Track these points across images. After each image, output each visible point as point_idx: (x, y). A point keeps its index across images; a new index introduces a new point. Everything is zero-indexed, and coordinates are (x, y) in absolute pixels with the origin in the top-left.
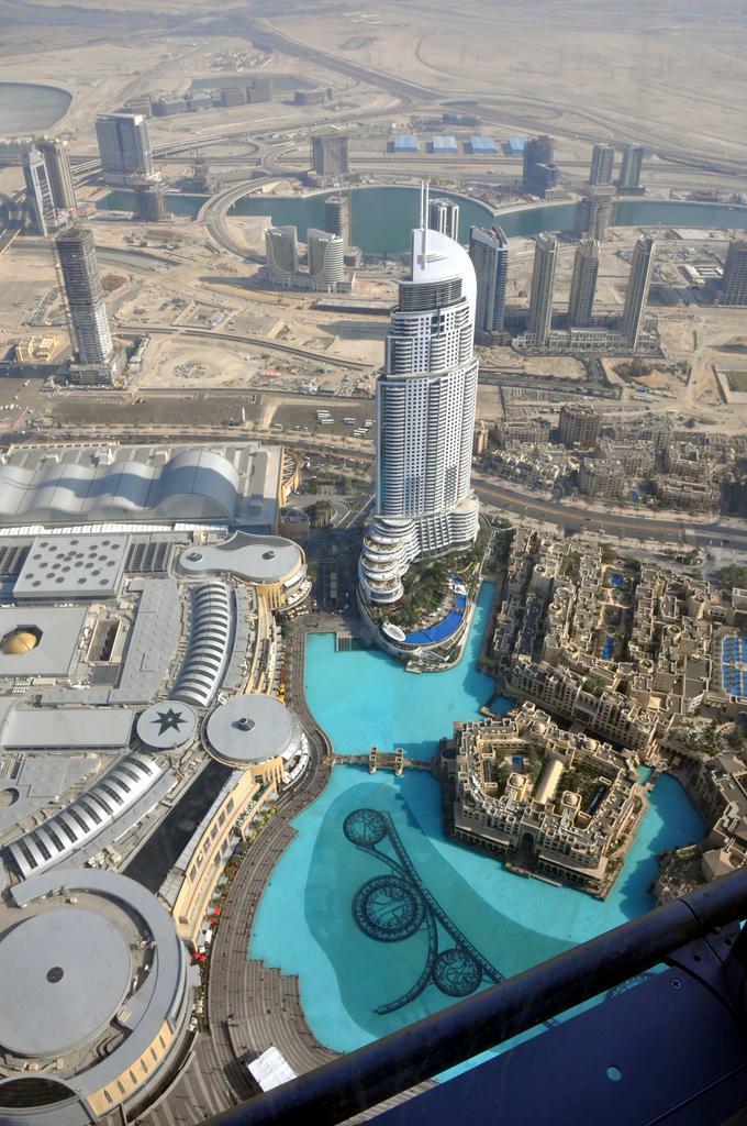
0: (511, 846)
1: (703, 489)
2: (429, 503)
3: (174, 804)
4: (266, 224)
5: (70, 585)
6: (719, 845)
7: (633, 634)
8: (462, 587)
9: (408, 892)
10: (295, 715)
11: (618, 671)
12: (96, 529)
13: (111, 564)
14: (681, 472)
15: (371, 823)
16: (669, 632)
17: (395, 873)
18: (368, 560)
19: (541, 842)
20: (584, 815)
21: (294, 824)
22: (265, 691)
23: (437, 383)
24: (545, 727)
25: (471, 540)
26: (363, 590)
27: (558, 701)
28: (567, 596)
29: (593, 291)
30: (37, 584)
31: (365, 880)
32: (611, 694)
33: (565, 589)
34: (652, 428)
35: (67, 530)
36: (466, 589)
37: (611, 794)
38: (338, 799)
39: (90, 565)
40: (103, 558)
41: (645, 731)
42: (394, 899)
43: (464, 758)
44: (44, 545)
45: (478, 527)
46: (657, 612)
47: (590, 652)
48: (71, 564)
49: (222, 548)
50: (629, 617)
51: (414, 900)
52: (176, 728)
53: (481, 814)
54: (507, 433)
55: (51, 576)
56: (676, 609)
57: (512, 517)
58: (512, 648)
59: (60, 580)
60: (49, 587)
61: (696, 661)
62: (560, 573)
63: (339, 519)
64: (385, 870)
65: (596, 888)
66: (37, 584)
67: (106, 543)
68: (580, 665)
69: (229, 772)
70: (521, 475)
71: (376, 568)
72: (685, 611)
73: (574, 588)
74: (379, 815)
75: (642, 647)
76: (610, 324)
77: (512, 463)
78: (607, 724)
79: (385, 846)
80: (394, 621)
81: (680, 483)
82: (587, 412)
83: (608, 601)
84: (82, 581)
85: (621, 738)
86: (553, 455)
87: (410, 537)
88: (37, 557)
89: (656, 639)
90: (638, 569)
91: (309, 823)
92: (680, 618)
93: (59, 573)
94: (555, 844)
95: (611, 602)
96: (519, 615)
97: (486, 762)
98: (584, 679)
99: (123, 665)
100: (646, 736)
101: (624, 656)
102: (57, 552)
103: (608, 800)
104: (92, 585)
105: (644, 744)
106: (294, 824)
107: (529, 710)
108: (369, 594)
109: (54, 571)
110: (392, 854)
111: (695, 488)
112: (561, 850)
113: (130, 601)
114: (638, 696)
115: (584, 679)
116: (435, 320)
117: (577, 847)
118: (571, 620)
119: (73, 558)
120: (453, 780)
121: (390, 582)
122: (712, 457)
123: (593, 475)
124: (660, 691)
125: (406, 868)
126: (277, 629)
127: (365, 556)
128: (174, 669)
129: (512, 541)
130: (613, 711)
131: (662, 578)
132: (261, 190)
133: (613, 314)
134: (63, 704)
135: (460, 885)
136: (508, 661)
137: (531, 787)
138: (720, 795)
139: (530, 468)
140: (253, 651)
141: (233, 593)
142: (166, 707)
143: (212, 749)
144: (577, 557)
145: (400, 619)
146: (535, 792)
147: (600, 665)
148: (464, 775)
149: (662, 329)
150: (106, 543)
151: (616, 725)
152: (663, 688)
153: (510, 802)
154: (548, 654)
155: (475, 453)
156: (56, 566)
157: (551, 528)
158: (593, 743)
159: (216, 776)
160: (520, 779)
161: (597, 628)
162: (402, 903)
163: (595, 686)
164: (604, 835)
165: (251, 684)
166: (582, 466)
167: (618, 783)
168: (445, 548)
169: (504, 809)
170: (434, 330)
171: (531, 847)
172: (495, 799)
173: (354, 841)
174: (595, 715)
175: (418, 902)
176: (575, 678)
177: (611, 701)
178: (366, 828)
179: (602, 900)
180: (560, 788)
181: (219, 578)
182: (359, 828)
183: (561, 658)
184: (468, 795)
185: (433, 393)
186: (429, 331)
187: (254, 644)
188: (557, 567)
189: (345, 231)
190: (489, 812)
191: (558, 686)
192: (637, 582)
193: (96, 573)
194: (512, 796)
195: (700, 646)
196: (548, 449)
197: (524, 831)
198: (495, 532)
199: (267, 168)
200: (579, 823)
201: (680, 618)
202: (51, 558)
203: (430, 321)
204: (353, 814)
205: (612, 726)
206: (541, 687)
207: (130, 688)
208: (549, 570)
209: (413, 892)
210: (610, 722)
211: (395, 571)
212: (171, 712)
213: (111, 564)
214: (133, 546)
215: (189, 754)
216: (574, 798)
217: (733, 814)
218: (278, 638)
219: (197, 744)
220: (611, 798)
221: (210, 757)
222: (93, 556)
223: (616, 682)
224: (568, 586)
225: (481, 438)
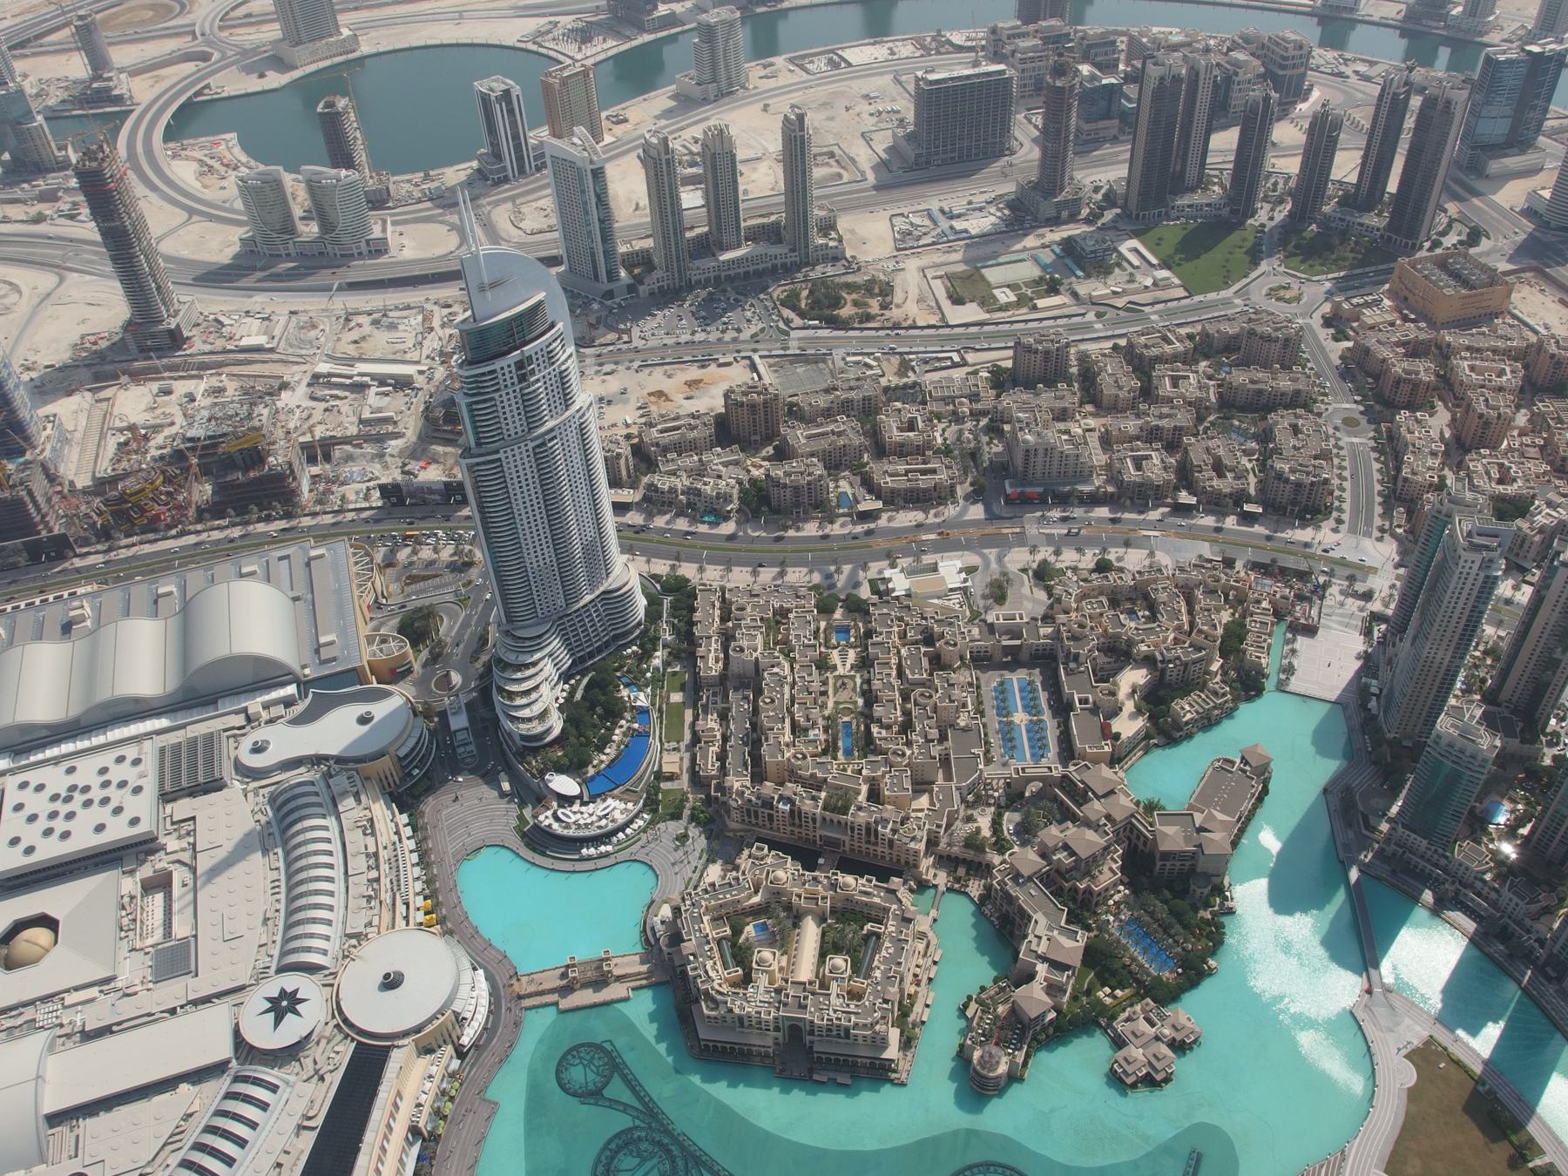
0: (777, 1044)
1: (934, 471)
2: (571, 596)
3: (319, 1122)
4: (229, 145)
5: (83, 839)
6: (1030, 977)
7: (876, 715)
8: (642, 696)
9: (659, 1143)
10: (453, 941)
11: (864, 772)
12: (97, 740)
13: (138, 790)
14: (902, 451)
15: (591, 1062)
16: (920, 700)
17: (637, 1122)
18: (511, 695)
19: (812, 1033)
20: (859, 983)
21: (491, 1094)
22: (406, 918)
23: (544, 444)
24: (786, 872)
25: (639, 624)
26: (509, 735)
27: (796, 830)
28: (781, 680)
29: (735, 182)
30: (30, 850)
31: (601, 1144)
32: (860, 809)
33: (776, 670)
34: (852, 394)
35: (50, 753)
36: (647, 697)
37: (887, 944)
38: (541, 1041)
39: (105, 801)
40: (123, 784)
41: (912, 845)
42: (644, 1160)
43: (688, 947)
44: (23, 785)
45: (645, 602)
46: (901, 674)
47: (825, 752)
48: (76, 805)
49: (296, 721)
50: (865, 687)
51: (668, 1151)
52: (297, 1013)
53: (729, 1016)
54: (657, 445)
55: (48, 832)
56: (925, 663)
57: (688, 570)
58: (723, 768)
59: (65, 835)
60: (51, 850)
61: (965, 730)
62: (766, 644)
63: (451, 628)
64: (623, 1121)
65: (895, 1071)
66: (30, 850)
67: (120, 760)
68: (813, 776)
69: (388, 1049)
70: (689, 505)
71: (519, 701)
72: (937, 662)
73: (787, 666)
74: (598, 1047)
75: (888, 727)
76: (770, 234)
77: (672, 490)
78: (864, 846)
79: (617, 1089)
80: (560, 770)
81: (901, 468)
82: (759, 394)
83: (835, 668)
84: (100, 828)
85: (885, 865)
86: (726, 464)
87: (556, 643)
88: (19, 807)
89: (907, 713)
90: (867, 613)
91: (510, 1089)
92: (931, 674)
93: (60, 825)
94: (829, 1030)
95: (841, 671)
96: (724, 717)
97: (719, 942)
98: (823, 794)
99: (195, 936)
100: (916, 852)
101: (868, 745)
102: (48, 793)
103: (884, 953)
104: (118, 831)
105: (916, 866)
106: (491, 1094)
107: (759, 854)
108: (517, 739)
109: (52, 824)
110: (627, 1097)
111: (924, 472)
112: (839, 1036)
113: (179, 838)
114: (898, 804)
115: (823, 794)
116: (520, 365)
117: (856, 1025)
118: (792, 714)
119: (76, 794)
120: (684, 973)
121: (543, 715)
122: (939, 417)
123: (785, 486)
124: (922, 785)
125: (650, 1111)
126: (404, 818)
127: (501, 690)
128: (270, 923)
129: (694, 610)
130: (868, 829)
131: (900, 619)
132: (207, 86)
133: (773, 218)
134: (119, 1024)
135: (723, 1111)
136: (721, 788)
137: (784, 964)
138: (1020, 907)
139: (698, 492)
140: (378, 868)
141: (329, 786)
142: (272, 988)
143: (351, 1026)
144: (783, 613)
145: (566, 761)
146: (792, 964)
147: (838, 769)
148: (695, 969)
149: (843, 224)
150: (120, 760)
151: (876, 844)
152: (927, 778)
153: (762, 989)
154: (771, 770)
155: (615, 483)
156: (53, 815)
157: (740, 577)
158: (850, 879)
159: (368, 1063)
160: (766, 954)
161: (826, 713)
162: (655, 1161)
163: (840, 803)
164: (886, 1001)
165: (387, 916)
166: (767, 476)
167: (892, 926)
168: (607, 645)
169: (756, 1002)
170: (522, 378)
171: (801, 1039)
172: (741, 991)
173: (574, 1095)
174: (847, 839)
175: (676, 1151)
176: (814, 798)
177: (862, 817)
178: (588, 1070)
179: (903, 1084)
180: (822, 956)
181: (302, 769)
182: (577, 1074)
183: (791, 774)
184: (706, 992)
185: (542, 454)
186: (515, 380)
187: (376, 855)
188: (759, 640)
189: (361, 156)
190: (737, 1011)
191: (792, 811)
192: (869, 634)
193: (118, 811)
194: (762, 980)
195: (964, 705)
196: (717, 458)
197: (787, 1024)
198: (667, 602)
199: (209, 43)
200: (855, 995)
201: (931, 674)
202: (38, 804)
203: (513, 368)
204: (564, 1057)
205: (872, 848)
206: (770, 816)
207: (212, 974)
208: (753, 645)
209: (666, 1141)
210: (868, 842)
211: (544, 698)
212: (283, 991)
213: (138, 790)
214: (162, 750)
215: (324, 1042)
216: (839, 961)
217: (1041, 929)
218: (408, 831)
219: (332, 1024)
220: (887, 949)
221: (353, 1040)
222: (106, 784)
223: (864, 788)
224: (778, 664)
225: (622, 461)
